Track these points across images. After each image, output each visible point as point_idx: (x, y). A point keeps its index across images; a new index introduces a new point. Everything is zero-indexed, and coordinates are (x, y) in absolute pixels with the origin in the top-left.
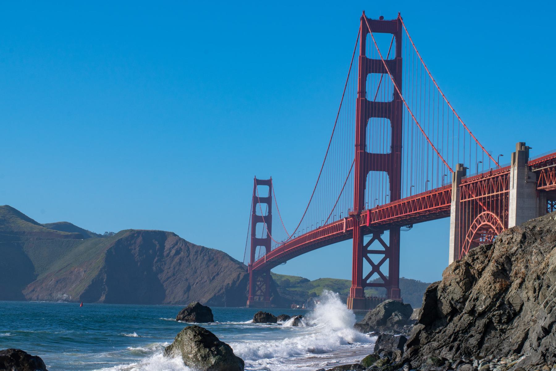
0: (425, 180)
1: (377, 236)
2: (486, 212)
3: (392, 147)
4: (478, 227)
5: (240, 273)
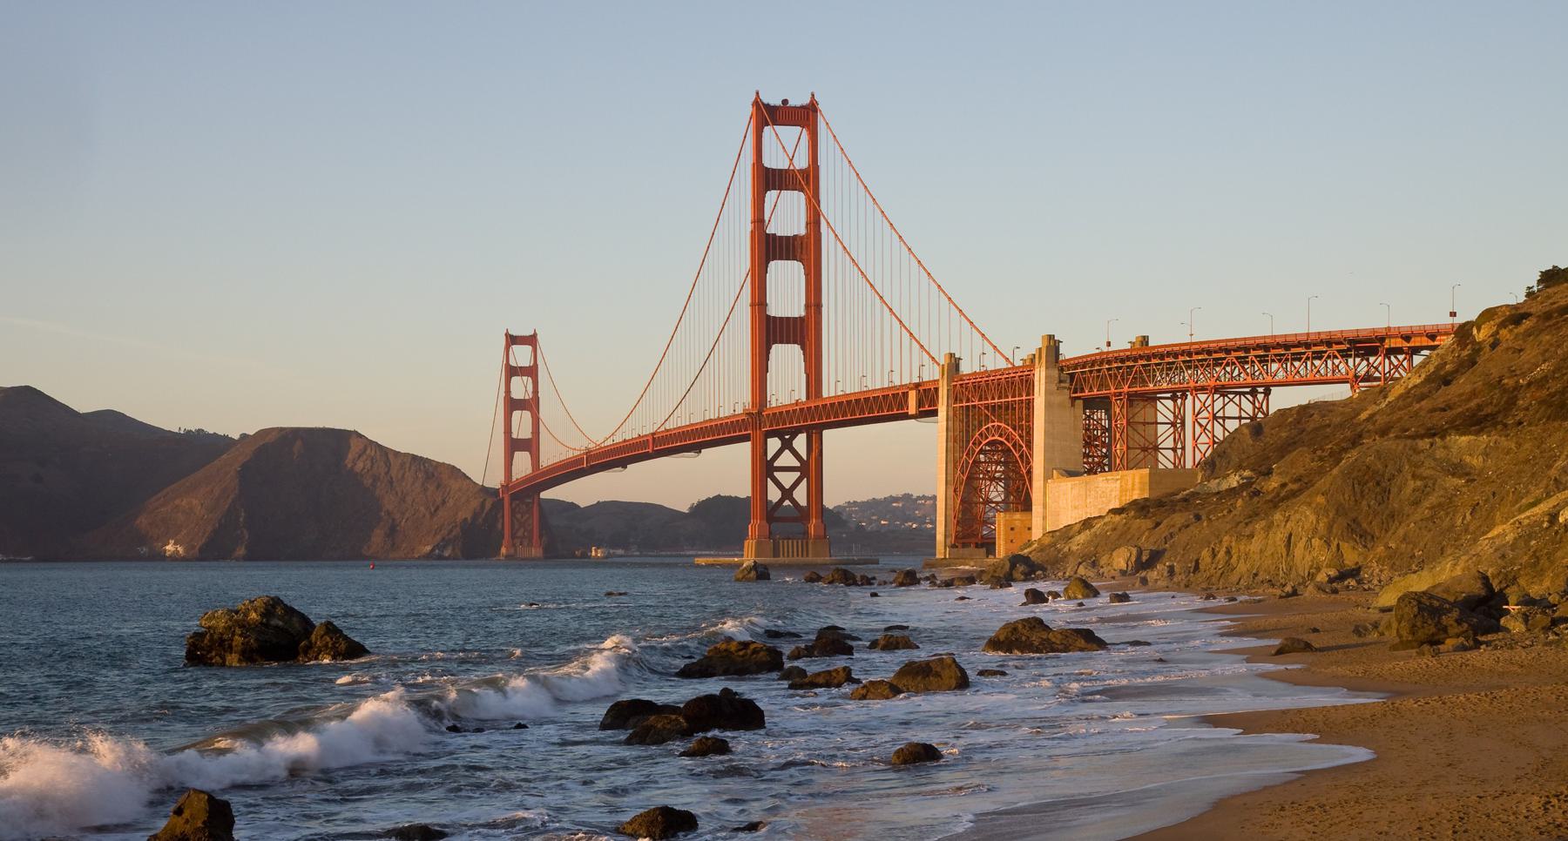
0: (887, 369)
1: (787, 445)
2: (996, 424)
3: (807, 306)
4: (984, 443)
5: (485, 500)
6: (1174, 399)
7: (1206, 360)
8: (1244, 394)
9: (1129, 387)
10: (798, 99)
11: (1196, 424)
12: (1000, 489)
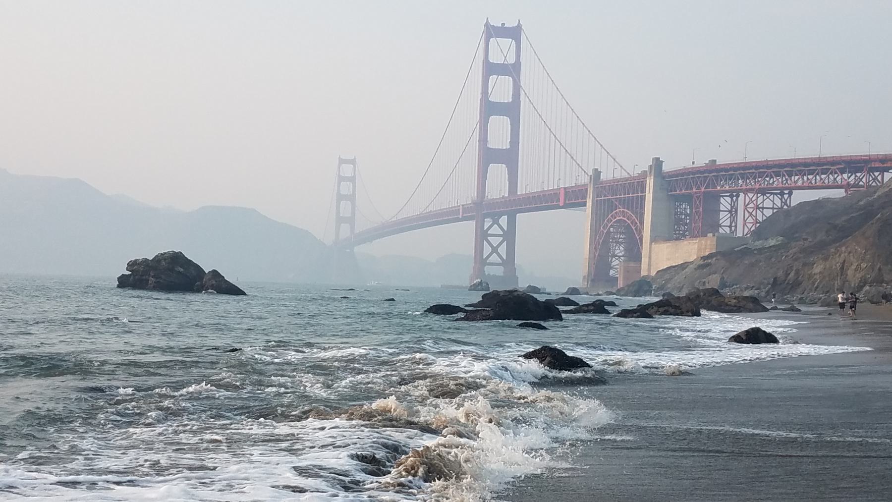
1: (496, 222)
6: (731, 197)
7: (754, 173)
8: (776, 194)
9: (705, 188)
10: (511, 23)
11: (746, 212)
12: (621, 248)
